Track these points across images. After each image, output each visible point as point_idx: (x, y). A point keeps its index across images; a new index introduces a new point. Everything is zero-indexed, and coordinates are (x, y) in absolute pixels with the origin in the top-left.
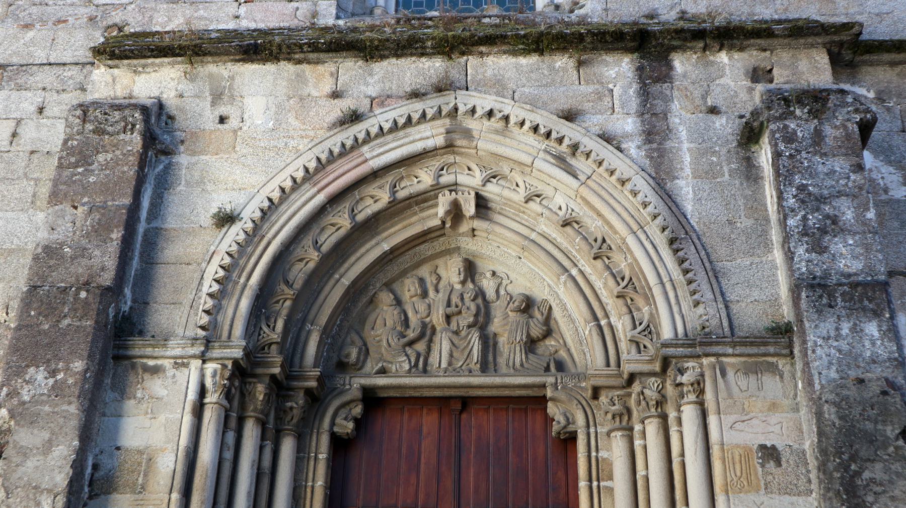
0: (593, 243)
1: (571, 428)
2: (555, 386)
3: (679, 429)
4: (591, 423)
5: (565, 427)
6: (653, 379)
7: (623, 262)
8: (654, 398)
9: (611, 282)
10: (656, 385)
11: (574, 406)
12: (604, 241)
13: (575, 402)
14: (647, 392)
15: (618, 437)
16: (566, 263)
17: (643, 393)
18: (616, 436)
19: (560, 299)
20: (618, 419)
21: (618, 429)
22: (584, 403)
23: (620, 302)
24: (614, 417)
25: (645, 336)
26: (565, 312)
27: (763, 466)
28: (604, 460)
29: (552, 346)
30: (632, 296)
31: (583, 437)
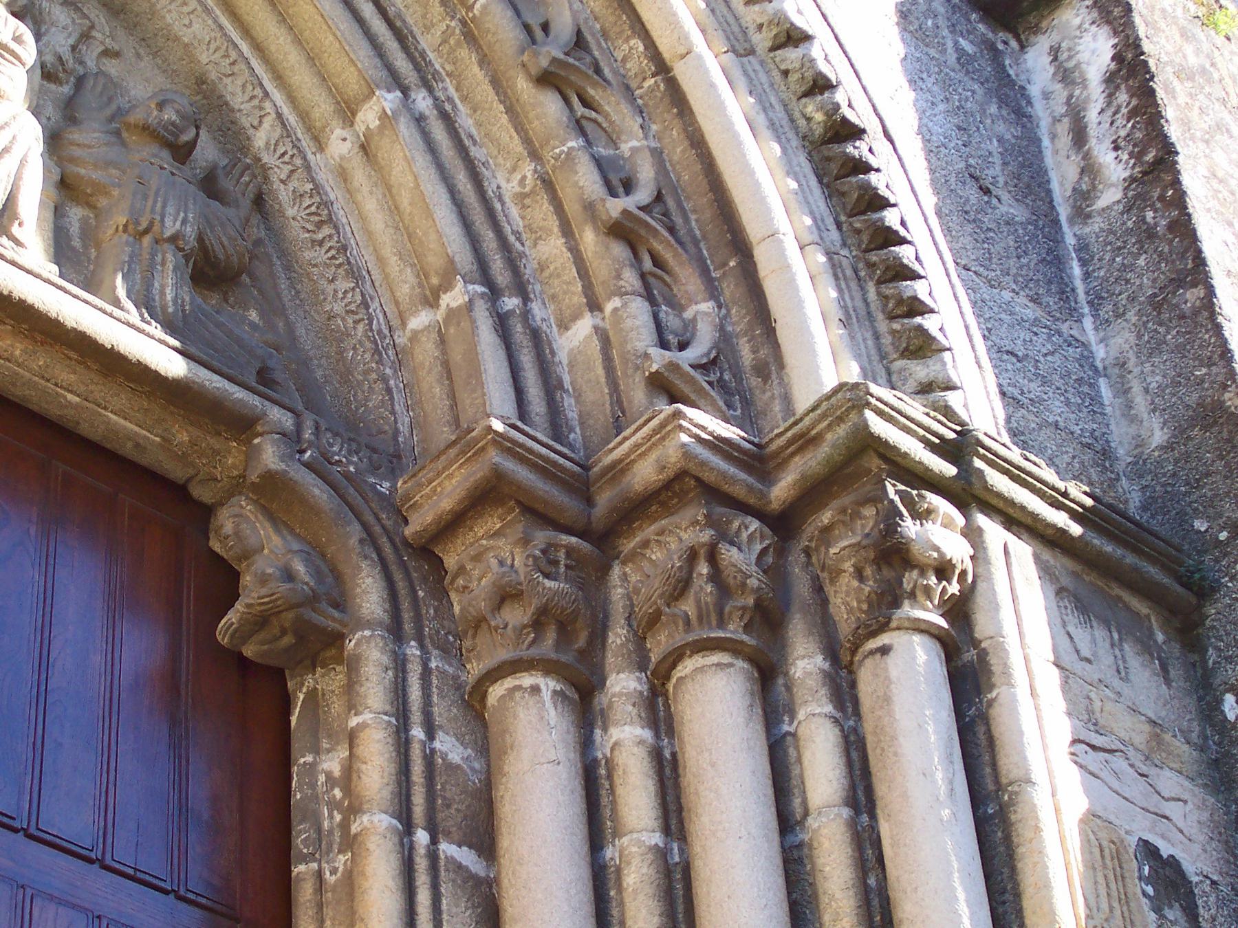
0: (539, 33)
1: (328, 619)
2: (292, 441)
3: (838, 715)
4: (408, 627)
5: (312, 600)
6: (754, 525)
7: (632, 136)
8: (753, 582)
9: (587, 179)
10: (758, 547)
11: (353, 542)
12: (579, 42)
13: (355, 531)
14: (731, 555)
15: (546, 695)
16: (402, 64)
17: (713, 557)
18: (535, 690)
19: (313, 180)
20: (550, 637)
21: (548, 667)
22: (388, 550)
23: (619, 250)
24: (537, 624)
25: (710, 383)
26: (326, 231)
27: (1158, 910)
28: (452, 768)
29: (253, 325)
30: (658, 247)
31: (385, 660)
